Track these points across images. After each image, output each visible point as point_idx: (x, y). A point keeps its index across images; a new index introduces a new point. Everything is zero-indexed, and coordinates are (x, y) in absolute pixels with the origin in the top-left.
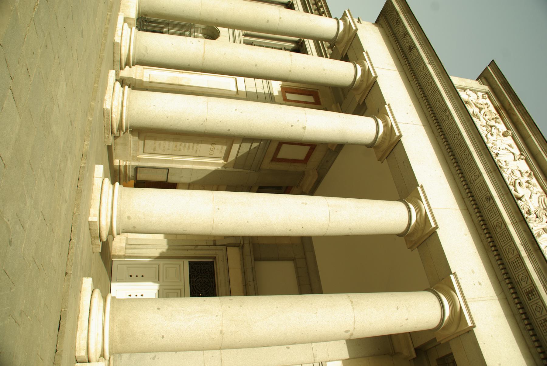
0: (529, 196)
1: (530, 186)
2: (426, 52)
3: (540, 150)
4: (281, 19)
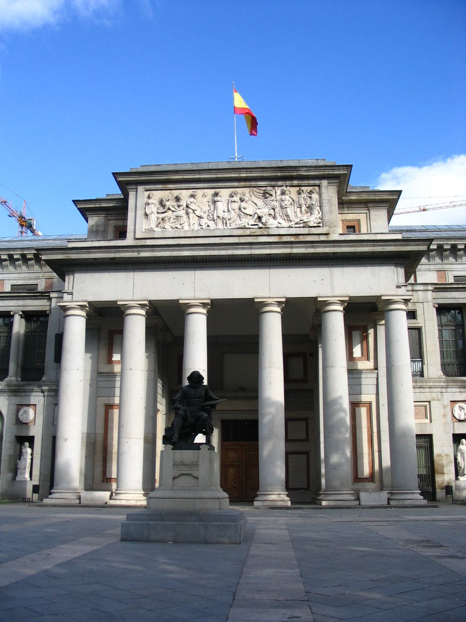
0: (254, 204)
1: (246, 199)
2: (125, 251)
3: (215, 176)
4: (79, 369)
